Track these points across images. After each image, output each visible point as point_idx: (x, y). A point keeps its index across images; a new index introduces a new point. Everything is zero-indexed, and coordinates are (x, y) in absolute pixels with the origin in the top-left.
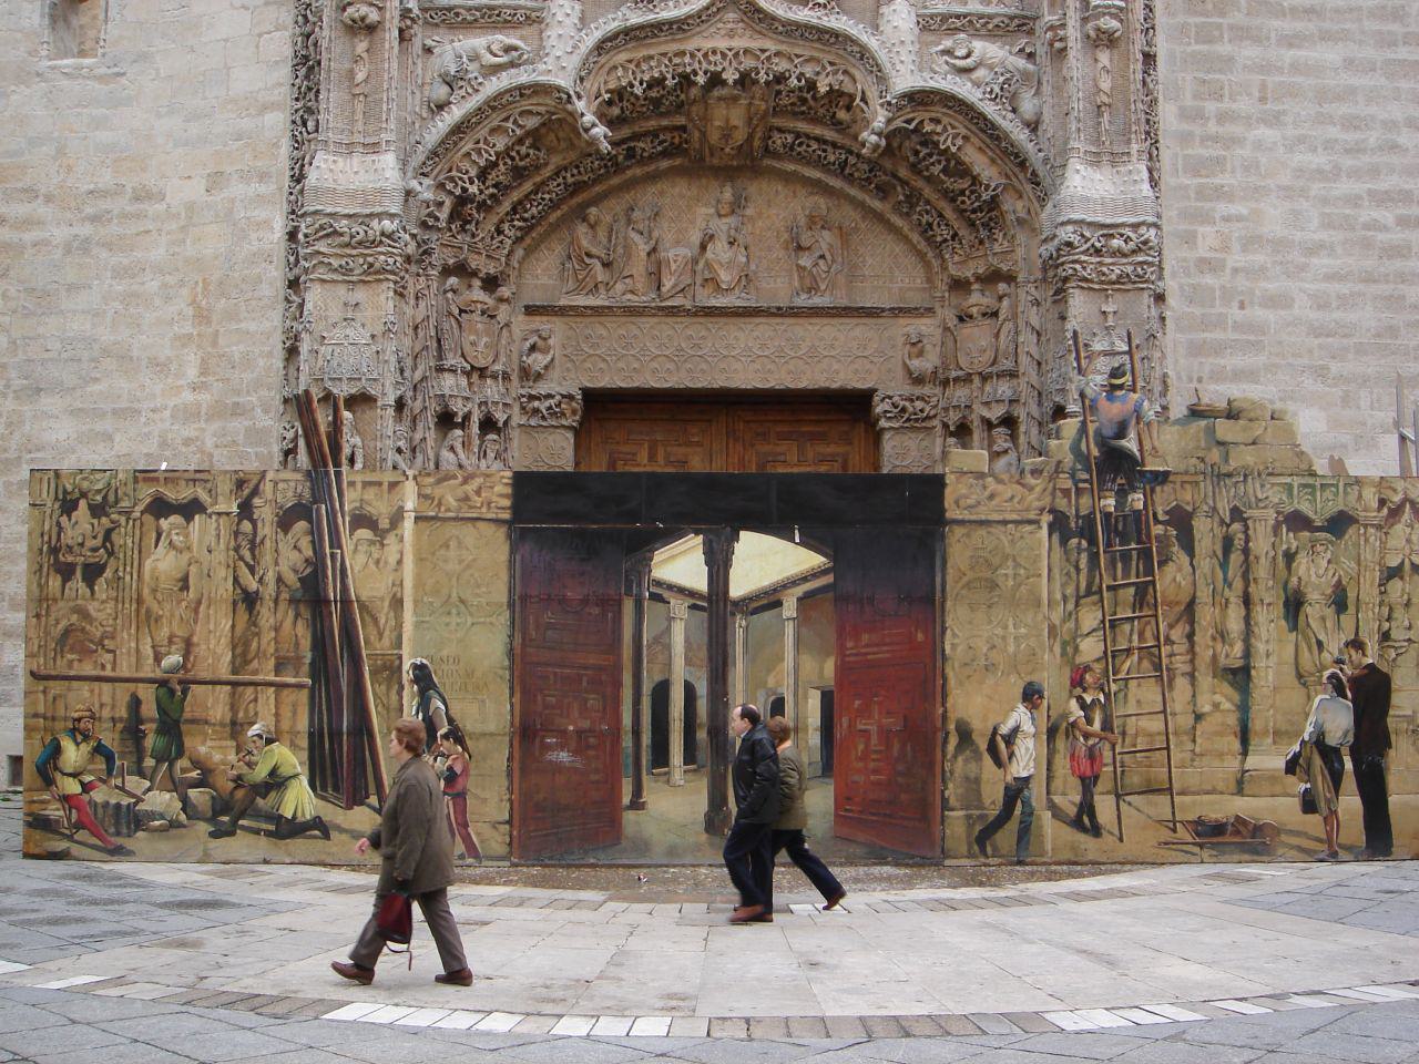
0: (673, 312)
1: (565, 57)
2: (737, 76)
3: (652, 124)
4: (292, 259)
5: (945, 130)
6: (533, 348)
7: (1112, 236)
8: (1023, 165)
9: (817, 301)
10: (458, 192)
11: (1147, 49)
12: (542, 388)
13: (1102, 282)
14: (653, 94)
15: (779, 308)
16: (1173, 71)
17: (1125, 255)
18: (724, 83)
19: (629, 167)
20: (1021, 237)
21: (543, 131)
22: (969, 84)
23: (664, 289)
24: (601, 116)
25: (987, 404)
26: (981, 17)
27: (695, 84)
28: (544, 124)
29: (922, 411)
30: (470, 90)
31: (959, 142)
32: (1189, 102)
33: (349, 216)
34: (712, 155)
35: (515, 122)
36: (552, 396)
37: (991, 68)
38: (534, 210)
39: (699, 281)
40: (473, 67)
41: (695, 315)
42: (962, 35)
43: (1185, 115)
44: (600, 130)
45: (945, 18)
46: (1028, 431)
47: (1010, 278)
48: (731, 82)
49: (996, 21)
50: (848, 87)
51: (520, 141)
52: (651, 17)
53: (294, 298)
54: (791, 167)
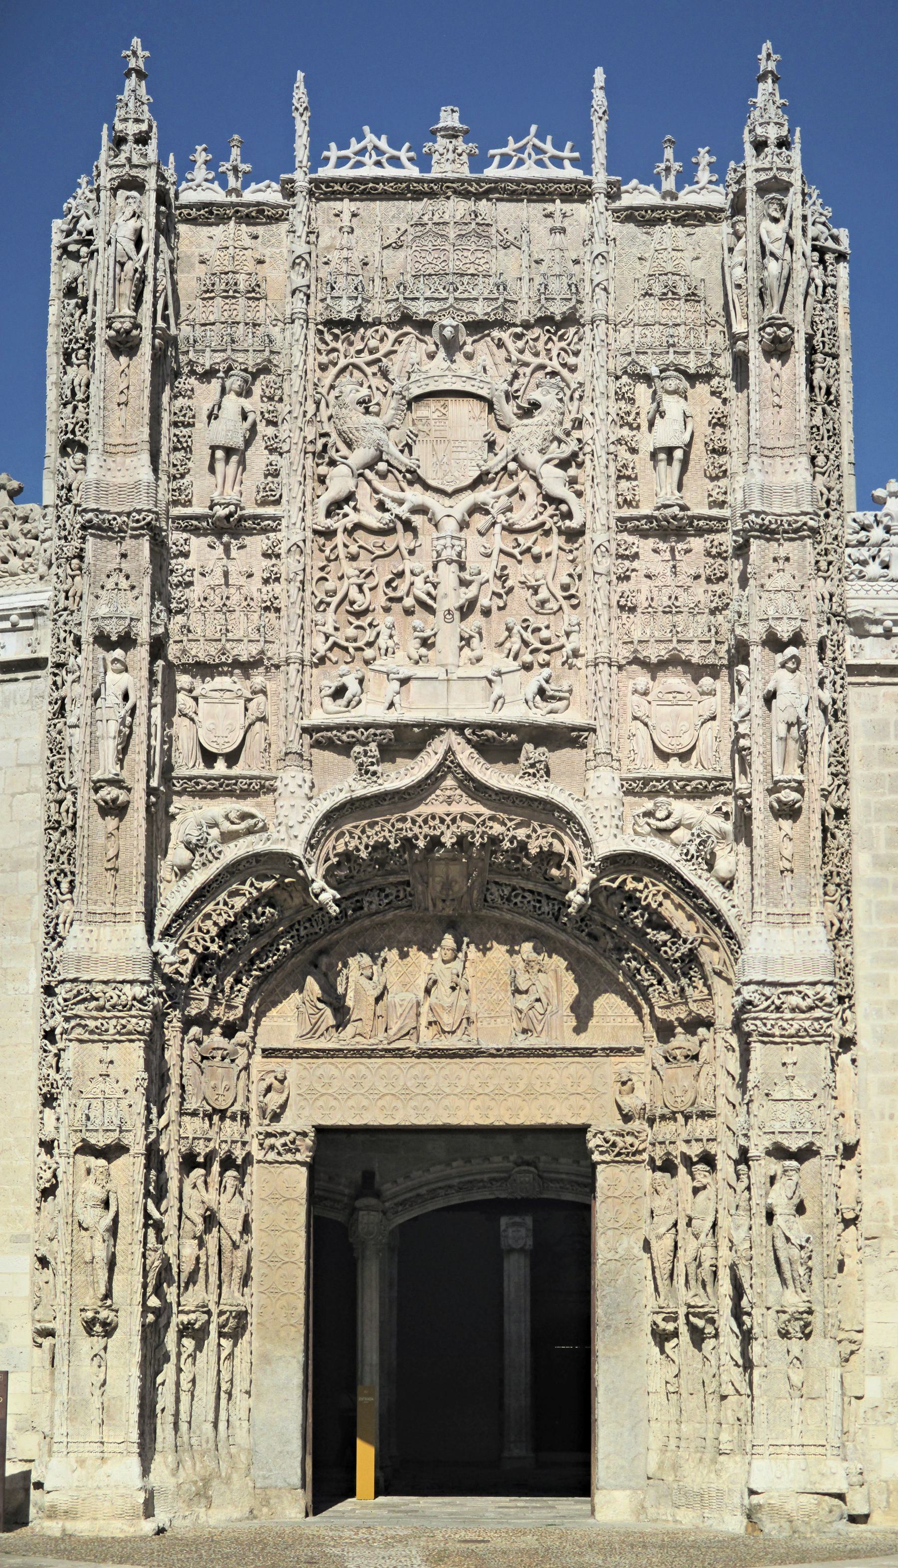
0: (400, 1053)
1: (297, 826)
2: (454, 840)
3: (379, 881)
4: (48, 1012)
5: (646, 886)
6: (269, 1089)
7: (791, 993)
8: (718, 920)
9: (533, 1042)
10: (200, 950)
11: (838, 804)
12: (277, 1127)
13: (782, 1036)
14: (377, 855)
15: (498, 1050)
16: (867, 822)
17: (803, 1012)
18: (443, 845)
19: (357, 919)
20: (718, 984)
21: (278, 892)
22: (667, 845)
23: (391, 1032)
24: (328, 876)
25: (688, 1142)
26: (680, 779)
27: (415, 847)
28: (277, 886)
29: (632, 1145)
30: (210, 857)
31: (660, 898)
32: (883, 850)
33: (106, 983)
34: (434, 905)
35: (252, 885)
36: (284, 1134)
37: (689, 827)
38: (270, 961)
39: (423, 1021)
40: (215, 832)
41: (419, 1057)
42: (662, 799)
43: (879, 863)
44: (328, 896)
45: (646, 781)
46: (725, 1166)
47: (708, 1024)
48: (448, 845)
49: (694, 783)
50: (557, 847)
51: (257, 901)
52: (373, 789)
53: (50, 1047)
54: (508, 916)
